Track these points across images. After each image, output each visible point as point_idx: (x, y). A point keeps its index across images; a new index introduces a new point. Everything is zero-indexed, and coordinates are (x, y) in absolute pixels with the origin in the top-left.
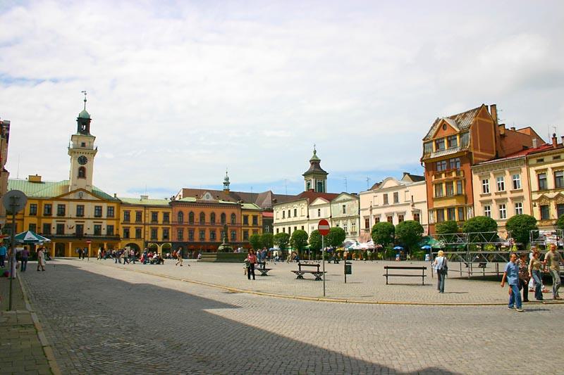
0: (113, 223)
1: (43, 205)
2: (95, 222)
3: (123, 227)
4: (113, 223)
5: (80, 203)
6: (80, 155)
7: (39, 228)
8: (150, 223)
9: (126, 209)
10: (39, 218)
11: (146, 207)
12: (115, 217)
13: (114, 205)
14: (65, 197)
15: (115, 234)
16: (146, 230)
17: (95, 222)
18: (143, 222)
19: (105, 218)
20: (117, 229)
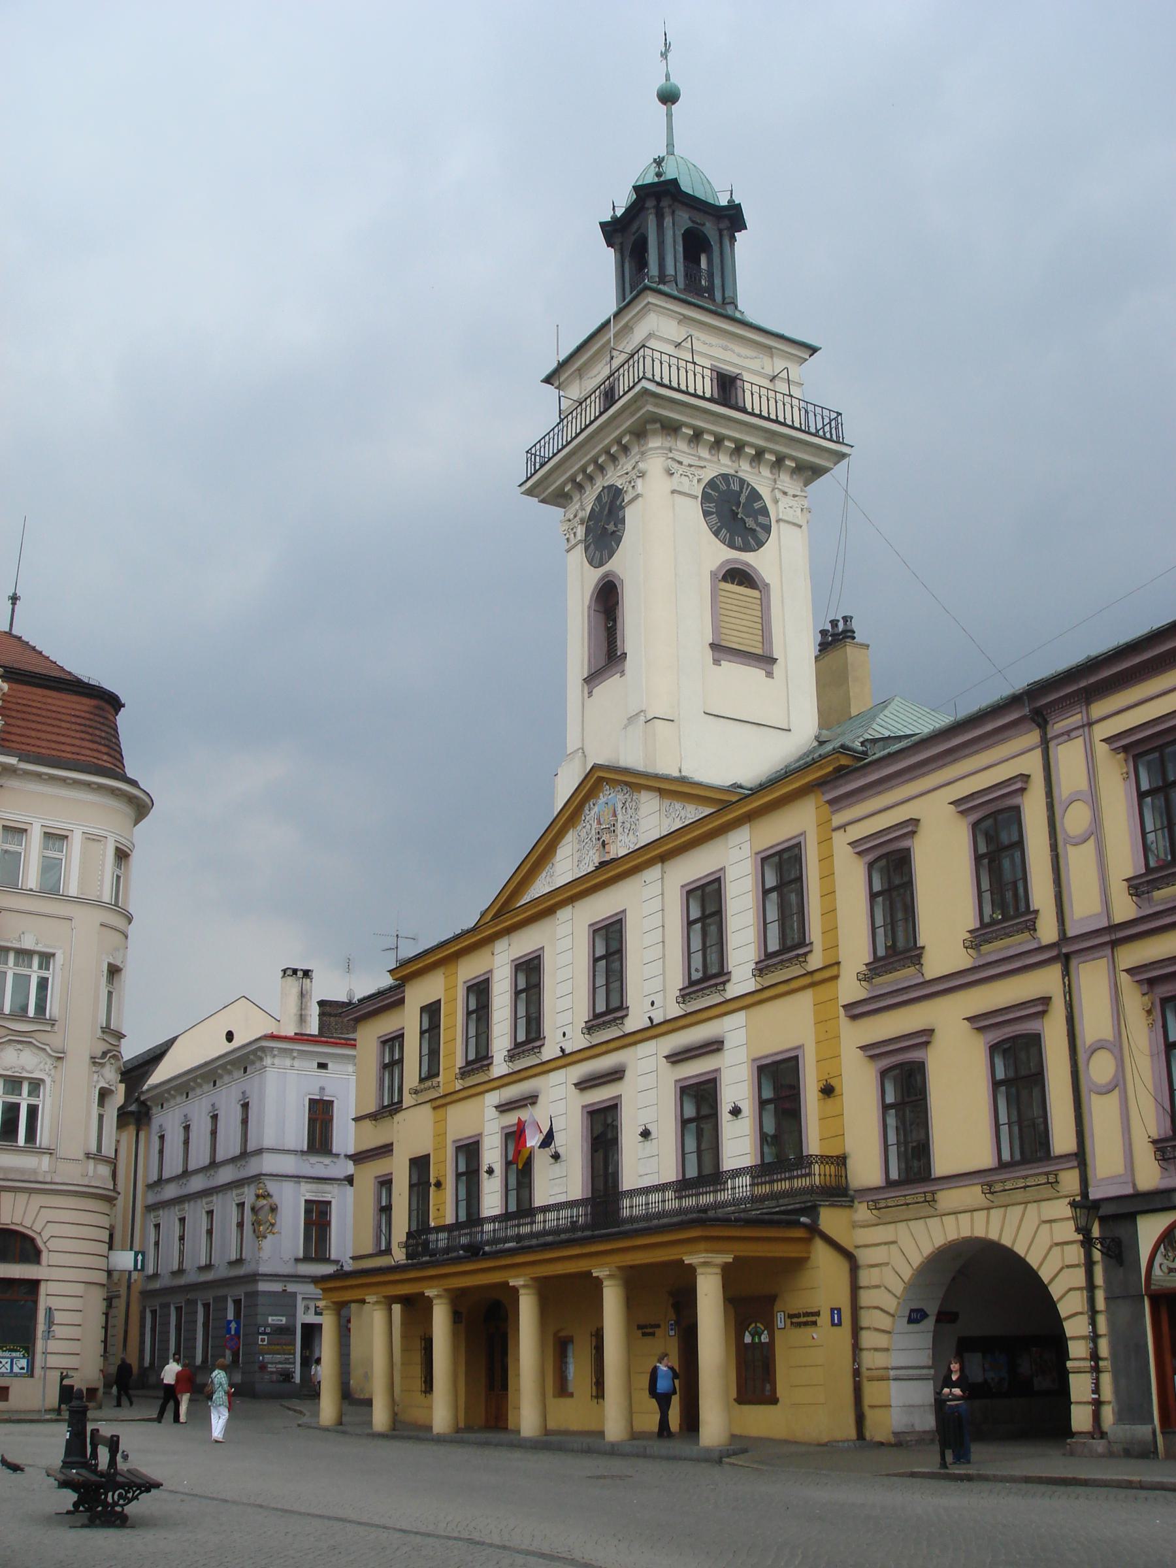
0: (789, 1025)
1: (461, 992)
2: (676, 1058)
3: (872, 1051)
4: (789, 1025)
5: (600, 907)
6: (588, 500)
7: (438, 1185)
8: (1125, 909)
9: (874, 816)
10: (441, 1104)
11: (1044, 704)
12: (815, 961)
13: (799, 821)
14: (541, 887)
15: (813, 1144)
16: (1095, 1022)
17: (676, 1058)
18: (1047, 932)
19: (750, 985)
20: (828, 1091)
